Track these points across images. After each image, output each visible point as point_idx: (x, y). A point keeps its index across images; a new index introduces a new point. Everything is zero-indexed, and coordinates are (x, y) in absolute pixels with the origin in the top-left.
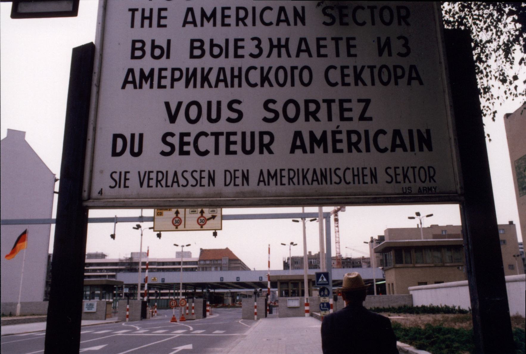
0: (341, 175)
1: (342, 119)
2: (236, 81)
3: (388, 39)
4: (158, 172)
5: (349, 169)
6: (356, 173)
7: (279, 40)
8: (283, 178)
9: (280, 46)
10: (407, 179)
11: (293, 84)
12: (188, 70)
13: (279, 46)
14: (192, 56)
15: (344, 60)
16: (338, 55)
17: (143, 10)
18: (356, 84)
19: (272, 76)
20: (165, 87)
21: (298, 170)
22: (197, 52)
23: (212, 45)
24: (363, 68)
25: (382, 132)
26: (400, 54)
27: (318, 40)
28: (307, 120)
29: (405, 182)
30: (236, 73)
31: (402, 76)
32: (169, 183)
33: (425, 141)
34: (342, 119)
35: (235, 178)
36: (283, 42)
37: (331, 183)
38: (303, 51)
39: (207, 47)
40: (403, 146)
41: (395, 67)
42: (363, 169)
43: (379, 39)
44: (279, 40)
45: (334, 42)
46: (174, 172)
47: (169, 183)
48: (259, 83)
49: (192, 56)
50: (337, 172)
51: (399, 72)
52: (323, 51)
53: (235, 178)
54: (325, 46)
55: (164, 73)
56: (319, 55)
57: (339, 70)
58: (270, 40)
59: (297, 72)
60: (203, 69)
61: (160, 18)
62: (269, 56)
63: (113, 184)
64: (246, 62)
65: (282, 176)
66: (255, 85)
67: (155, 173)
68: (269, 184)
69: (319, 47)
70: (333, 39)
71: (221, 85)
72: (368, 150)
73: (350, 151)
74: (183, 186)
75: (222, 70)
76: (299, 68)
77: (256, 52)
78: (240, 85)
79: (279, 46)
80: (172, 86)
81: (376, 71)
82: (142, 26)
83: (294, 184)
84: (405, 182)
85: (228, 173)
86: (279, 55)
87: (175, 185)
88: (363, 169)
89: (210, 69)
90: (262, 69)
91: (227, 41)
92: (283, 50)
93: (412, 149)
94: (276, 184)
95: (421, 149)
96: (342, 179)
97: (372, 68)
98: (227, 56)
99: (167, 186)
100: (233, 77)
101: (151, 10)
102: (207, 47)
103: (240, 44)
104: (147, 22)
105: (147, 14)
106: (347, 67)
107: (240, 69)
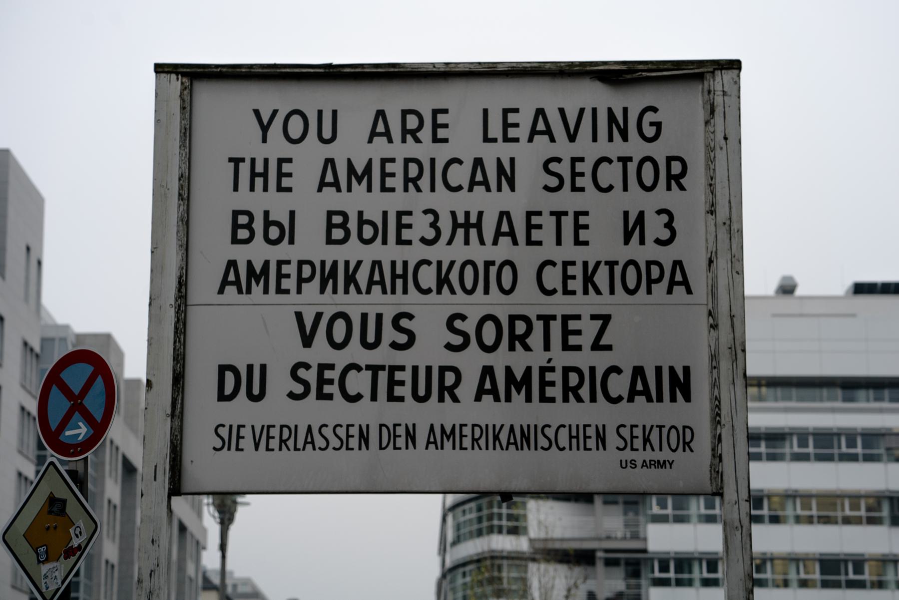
2: (399, 282)
3: (641, 214)
4: (282, 427)
5: (564, 426)
6: (574, 433)
7: (467, 214)
8: (464, 439)
9: (468, 225)
10: (648, 445)
11: (486, 291)
12: (323, 263)
13: (467, 226)
14: (330, 241)
15: (569, 251)
16: (559, 242)
17: (253, 161)
18: (586, 292)
19: (454, 277)
21: (487, 426)
22: (338, 234)
23: (362, 222)
24: (598, 264)
25: (616, 370)
26: (658, 241)
27: (529, 214)
29: (644, 449)
30: (399, 271)
31: (659, 280)
32: (300, 445)
33: (681, 385)
36: (473, 220)
37: (536, 449)
38: (505, 234)
39: (353, 225)
40: (646, 393)
41: (649, 264)
43: (626, 214)
44: (467, 214)
45: (554, 218)
47: (300, 445)
48: (434, 288)
49: (330, 241)
50: (547, 430)
51: (655, 272)
52: (536, 235)
53: (395, 436)
54: (539, 227)
55: (285, 269)
56: (530, 242)
57: (559, 267)
58: (453, 214)
59: (493, 270)
60: (347, 263)
61: (281, 175)
62: (450, 243)
63: (219, 444)
64: (414, 253)
65: (462, 436)
66: (428, 291)
67: (278, 429)
68: (442, 448)
69: (530, 227)
70: (552, 213)
71: (376, 289)
72: (593, 399)
73: (566, 399)
74: (320, 449)
75: (376, 264)
76: (497, 264)
77: (430, 234)
78: (405, 291)
79: (467, 226)
80: (299, 291)
81: (618, 270)
82: (252, 189)
83: (480, 449)
84: (644, 449)
85: (384, 429)
86: (467, 242)
87: (309, 446)
88: (585, 426)
89: (359, 263)
90: (439, 263)
91: (385, 214)
92: (473, 232)
93: (660, 399)
94: (454, 448)
95: (673, 399)
97: (611, 264)
98: (385, 242)
99: (296, 449)
100: (394, 276)
101: (266, 161)
102: (353, 225)
103: (405, 220)
104: (259, 181)
105: (259, 168)
106: (573, 263)
107: (405, 263)
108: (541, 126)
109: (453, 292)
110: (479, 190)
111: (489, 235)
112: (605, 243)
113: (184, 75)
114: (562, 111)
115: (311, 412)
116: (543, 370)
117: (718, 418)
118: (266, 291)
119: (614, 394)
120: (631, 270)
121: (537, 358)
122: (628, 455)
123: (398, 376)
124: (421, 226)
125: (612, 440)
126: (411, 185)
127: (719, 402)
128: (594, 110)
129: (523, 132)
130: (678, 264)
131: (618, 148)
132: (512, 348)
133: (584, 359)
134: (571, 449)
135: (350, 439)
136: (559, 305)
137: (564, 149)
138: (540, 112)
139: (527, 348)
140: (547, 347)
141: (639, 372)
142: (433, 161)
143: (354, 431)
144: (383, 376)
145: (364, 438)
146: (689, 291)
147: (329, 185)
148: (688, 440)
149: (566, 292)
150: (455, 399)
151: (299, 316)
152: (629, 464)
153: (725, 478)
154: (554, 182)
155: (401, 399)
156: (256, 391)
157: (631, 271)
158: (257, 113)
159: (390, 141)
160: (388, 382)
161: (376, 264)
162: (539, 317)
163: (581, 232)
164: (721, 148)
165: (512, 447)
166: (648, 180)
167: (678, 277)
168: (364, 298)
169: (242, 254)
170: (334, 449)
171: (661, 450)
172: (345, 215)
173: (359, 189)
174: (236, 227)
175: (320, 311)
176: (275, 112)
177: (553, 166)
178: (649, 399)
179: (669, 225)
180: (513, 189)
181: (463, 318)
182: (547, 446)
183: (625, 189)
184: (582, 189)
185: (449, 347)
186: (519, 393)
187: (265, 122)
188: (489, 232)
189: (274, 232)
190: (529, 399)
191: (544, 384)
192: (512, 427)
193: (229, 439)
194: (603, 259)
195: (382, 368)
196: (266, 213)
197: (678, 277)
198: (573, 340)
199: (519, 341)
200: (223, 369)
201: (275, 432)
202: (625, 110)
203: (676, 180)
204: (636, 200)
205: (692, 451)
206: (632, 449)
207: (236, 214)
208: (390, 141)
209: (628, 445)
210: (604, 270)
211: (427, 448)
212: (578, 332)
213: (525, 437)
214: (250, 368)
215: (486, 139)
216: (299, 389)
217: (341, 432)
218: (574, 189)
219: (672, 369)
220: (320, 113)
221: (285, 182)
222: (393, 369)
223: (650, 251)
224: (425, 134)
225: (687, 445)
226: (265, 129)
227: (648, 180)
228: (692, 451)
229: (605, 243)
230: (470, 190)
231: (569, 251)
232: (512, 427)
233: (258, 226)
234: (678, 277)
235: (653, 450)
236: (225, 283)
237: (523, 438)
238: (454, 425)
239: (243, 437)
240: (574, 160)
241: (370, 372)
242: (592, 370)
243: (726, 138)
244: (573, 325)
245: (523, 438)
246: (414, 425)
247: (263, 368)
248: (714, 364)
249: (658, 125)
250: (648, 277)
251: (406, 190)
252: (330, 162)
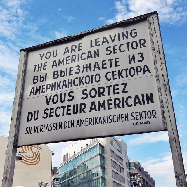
2: (70, 84)
3: (134, 56)
5: (115, 115)
6: (118, 117)
7: (87, 65)
9: (87, 67)
11: (92, 82)
12: (52, 84)
13: (87, 67)
15: (114, 68)
16: (111, 67)
17: (39, 65)
18: (119, 78)
20: (44, 92)
21: (93, 118)
23: (61, 72)
24: (122, 70)
25: (130, 97)
26: (139, 61)
27: (103, 62)
29: (140, 119)
30: (70, 82)
33: (150, 99)
35: (68, 124)
36: (88, 66)
37: (107, 123)
40: (140, 102)
41: (137, 67)
42: (121, 114)
43: (129, 56)
44: (87, 65)
48: (79, 84)
49: (54, 78)
50: (110, 117)
51: (139, 69)
52: (105, 66)
53: (68, 124)
56: (103, 68)
57: (112, 73)
58: (83, 65)
59: (94, 77)
60: (58, 82)
61: (44, 66)
62: (82, 72)
65: (86, 122)
67: (40, 126)
68: (81, 126)
69: (103, 64)
70: (109, 60)
71: (64, 87)
72: (124, 106)
73: (115, 108)
74: (50, 130)
75: (65, 81)
76: (95, 75)
77: (78, 71)
81: (128, 71)
84: (140, 119)
85: (66, 123)
86: (87, 71)
89: (61, 82)
90: (80, 78)
92: (88, 69)
93: (144, 103)
94: (84, 125)
95: (148, 103)
97: (126, 70)
104: (40, 69)
105: (40, 66)
106: (115, 71)
107: (71, 80)
109: (83, 84)
110: (90, 58)
111: (92, 68)
112: (124, 64)
113: (25, 50)
114: (110, 36)
115: (49, 121)
116: (108, 101)
117: (162, 106)
119: (129, 104)
120: (132, 70)
121: (106, 98)
122: (135, 121)
123: (69, 108)
125: (130, 117)
126: (73, 61)
127: (162, 101)
128: (119, 34)
129: (100, 43)
131: (126, 41)
132: (99, 96)
133: (120, 96)
134: (118, 122)
135: (57, 127)
136: (112, 83)
137: (111, 44)
138: (105, 38)
139: (104, 95)
140: (109, 94)
141: (137, 97)
143: (58, 124)
144: (66, 109)
145: (61, 126)
146: (150, 72)
148: (154, 114)
149: (114, 79)
150: (84, 112)
151: (46, 97)
152: (136, 124)
153: (167, 124)
154: (109, 52)
155: (70, 114)
156: (36, 118)
157: (132, 70)
158: (40, 55)
159: (69, 53)
160: (67, 110)
162: (107, 87)
164: (154, 33)
165: (100, 123)
167: (146, 69)
168: (61, 90)
170: (53, 130)
171: (146, 118)
175: (51, 95)
177: (108, 49)
178: (141, 104)
179: (142, 56)
180: (98, 56)
181: (86, 90)
182: (110, 121)
183: (128, 50)
185: (83, 98)
188: (92, 68)
189: (42, 79)
190: (105, 109)
191: (109, 104)
192: (100, 117)
193: (29, 131)
195: (65, 107)
197: (146, 69)
198: (116, 91)
199: (101, 94)
200: (29, 113)
201: (39, 127)
204: (132, 52)
205: (156, 117)
206: (137, 119)
208: (69, 53)
209: (135, 118)
210: (124, 72)
211: (77, 126)
212: (118, 89)
213: (104, 120)
214: (35, 112)
215: (91, 47)
216: (45, 115)
217: (55, 125)
218: (114, 53)
219: (147, 95)
222: (68, 106)
223: (137, 64)
224: (77, 49)
225: (154, 116)
226: (42, 57)
228: (156, 117)
229: (124, 64)
230: (88, 59)
231: (114, 68)
232: (100, 117)
234: (146, 69)
235: (143, 119)
236: (31, 93)
237: (104, 120)
238: (84, 119)
239: (32, 130)
240: (114, 46)
241: (62, 108)
242: (123, 98)
243: (155, 30)
244: (116, 87)
245: (104, 120)
247: (38, 111)
248: (159, 90)
249: (136, 33)
250: (137, 71)
251: (72, 62)
252: (55, 61)
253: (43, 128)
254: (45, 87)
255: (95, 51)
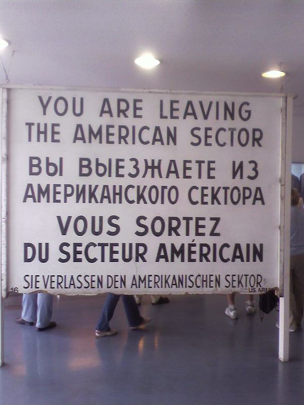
0: (194, 281)
1: (198, 234)
2: (117, 197)
7: (153, 161)
9: (153, 167)
10: (240, 284)
11: (162, 203)
12: (78, 186)
13: (153, 167)
14: (81, 174)
15: (205, 182)
16: (200, 177)
17: (39, 125)
18: (213, 203)
20: (59, 201)
22: (85, 171)
24: (219, 188)
25: (227, 245)
26: (250, 177)
27: (185, 162)
28: (170, 234)
30: (117, 191)
32: (67, 286)
33: (258, 253)
34: (198, 234)
36: (156, 164)
38: (173, 172)
39: (93, 166)
40: (241, 257)
41: (245, 188)
44: (153, 161)
46: (71, 276)
48: (136, 200)
49: (81, 174)
52: (188, 173)
54: (190, 169)
56: (185, 177)
57: (200, 190)
58: (146, 161)
59: (166, 191)
60: (90, 186)
62: (144, 176)
64: (125, 182)
65: (149, 281)
66: (132, 202)
68: (139, 287)
69: (185, 169)
70: (197, 162)
71: (106, 200)
72: (215, 260)
73: (201, 261)
75: (106, 187)
76: (168, 188)
77: (134, 172)
79: (153, 167)
80: (65, 202)
81: (229, 192)
82: (38, 140)
86: (153, 176)
89: (97, 187)
90: (138, 187)
91: (110, 160)
92: (156, 171)
93: (248, 260)
95: (254, 260)
96: (194, 283)
97: (226, 189)
98: (110, 176)
100: (115, 194)
101: (46, 125)
102: (93, 166)
103: (121, 164)
105: (42, 129)
106: (206, 188)
107: (121, 187)
108: (190, 111)
109: (145, 203)
111: (164, 173)
114: (201, 103)
116: (190, 245)
118: (48, 201)
120: (236, 192)
124: (129, 168)
128: (217, 104)
129: (181, 113)
130: (258, 189)
131: (228, 124)
137: (201, 123)
138: (190, 103)
141: (238, 246)
142: (134, 128)
146: (263, 204)
147: (80, 139)
149: (204, 203)
156: (44, 257)
157: (236, 192)
158: (40, 98)
159: (111, 116)
160: (111, 252)
161: (106, 187)
163: (211, 171)
166: (243, 141)
167: (259, 197)
169: (35, 181)
170: (85, 287)
172: (89, 160)
173: (95, 141)
174: (31, 166)
176: (50, 98)
177: (196, 132)
179: (255, 169)
180: (175, 144)
183: (232, 145)
184: (210, 145)
186: (178, 257)
187: (45, 102)
190: (183, 260)
191: (190, 252)
192: (174, 276)
194: (222, 186)
196: (47, 159)
197: (259, 197)
202: (233, 104)
203: (257, 141)
207: (31, 159)
208: (111, 116)
210: (222, 192)
213: (181, 281)
214: (40, 245)
215: (162, 117)
217: (88, 279)
218: (207, 144)
219: (254, 246)
220: (74, 99)
221: (56, 137)
224: (130, 113)
226: (45, 107)
227: (243, 141)
229: (223, 178)
230: (153, 144)
231: (205, 182)
233: (43, 165)
234: (258, 196)
236: (27, 196)
238: (145, 276)
240: (207, 129)
242: (215, 245)
246: (125, 276)
247: (47, 245)
249: (249, 112)
252: (79, 127)
253: (64, 282)
254: (61, 189)
255: (168, 129)
